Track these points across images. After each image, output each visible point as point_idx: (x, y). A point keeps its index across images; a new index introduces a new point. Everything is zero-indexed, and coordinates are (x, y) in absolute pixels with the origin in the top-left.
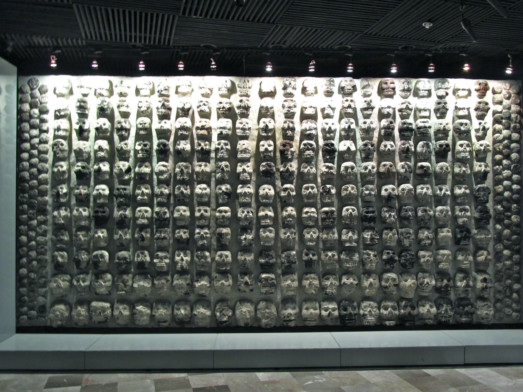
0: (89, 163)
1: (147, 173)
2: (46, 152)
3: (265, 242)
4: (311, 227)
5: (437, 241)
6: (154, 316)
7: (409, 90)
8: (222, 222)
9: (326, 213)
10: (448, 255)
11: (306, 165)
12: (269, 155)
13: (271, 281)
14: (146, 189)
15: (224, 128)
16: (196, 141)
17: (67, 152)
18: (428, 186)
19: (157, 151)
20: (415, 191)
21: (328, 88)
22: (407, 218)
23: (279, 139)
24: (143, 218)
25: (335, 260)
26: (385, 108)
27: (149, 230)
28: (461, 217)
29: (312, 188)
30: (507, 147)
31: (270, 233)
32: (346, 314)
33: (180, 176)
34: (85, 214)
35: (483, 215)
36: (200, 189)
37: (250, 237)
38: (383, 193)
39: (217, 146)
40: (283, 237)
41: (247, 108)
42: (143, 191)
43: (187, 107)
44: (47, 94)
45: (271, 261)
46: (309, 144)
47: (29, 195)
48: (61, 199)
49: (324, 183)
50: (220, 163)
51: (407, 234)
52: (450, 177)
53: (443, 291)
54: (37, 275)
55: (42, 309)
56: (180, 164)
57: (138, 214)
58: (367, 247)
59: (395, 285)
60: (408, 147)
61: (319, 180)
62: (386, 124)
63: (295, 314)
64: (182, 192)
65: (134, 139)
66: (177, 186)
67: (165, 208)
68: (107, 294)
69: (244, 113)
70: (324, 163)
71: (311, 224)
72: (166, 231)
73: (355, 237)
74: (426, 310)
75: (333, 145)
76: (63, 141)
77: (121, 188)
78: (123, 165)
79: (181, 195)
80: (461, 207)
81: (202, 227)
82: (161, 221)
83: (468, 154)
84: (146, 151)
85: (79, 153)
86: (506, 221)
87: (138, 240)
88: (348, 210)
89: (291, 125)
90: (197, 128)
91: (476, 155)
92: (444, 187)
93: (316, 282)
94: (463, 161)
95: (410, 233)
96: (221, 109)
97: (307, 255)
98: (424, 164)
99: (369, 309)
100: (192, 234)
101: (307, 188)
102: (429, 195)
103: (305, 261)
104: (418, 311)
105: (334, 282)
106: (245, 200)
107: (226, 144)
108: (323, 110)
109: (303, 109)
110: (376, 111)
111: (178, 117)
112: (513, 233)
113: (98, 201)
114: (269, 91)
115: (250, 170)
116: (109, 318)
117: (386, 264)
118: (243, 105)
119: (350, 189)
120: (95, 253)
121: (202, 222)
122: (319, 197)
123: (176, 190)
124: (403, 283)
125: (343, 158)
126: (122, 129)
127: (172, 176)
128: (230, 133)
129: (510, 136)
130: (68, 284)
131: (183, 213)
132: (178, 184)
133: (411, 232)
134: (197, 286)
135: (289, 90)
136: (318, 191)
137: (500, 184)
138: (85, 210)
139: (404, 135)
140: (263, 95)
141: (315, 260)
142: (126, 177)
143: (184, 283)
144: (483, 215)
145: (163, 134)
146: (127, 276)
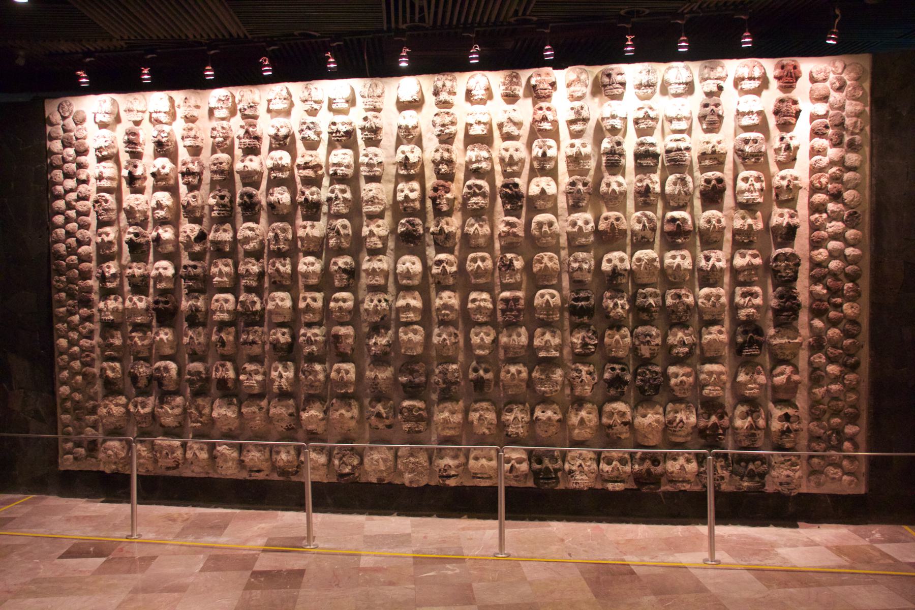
0: (145, 228)
1: (226, 242)
2: (87, 214)
3: (407, 349)
4: (481, 324)
5: (702, 349)
6: (243, 461)
7: (649, 85)
8: (340, 317)
9: (506, 301)
10: (721, 373)
12: (412, 207)
13: (417, 411)
14: (226, 265)
15: (339, 165)
16: (299, 186)
17: (115, 212)
18: (685, 252)
19: (239, 205)
20: (662, 262)
21: (507, 89)
22: (647, 309)
23: (430, 178)
24: (222, 311)
25: (522, 380)
26: (608, 118)
27: (232, 329)
28: (743, 307)
29: (483, 259)
30: (835, 179)
32: (540, 469)
34: (142, 305)
35: (785, 303)
36: (305, 264)
37: (383, 341)
38: (606, 266)
39: (331, 195)
41: (376, 130)
42: (220, 270)
43: (283, 132)
44: (85, 125)
45: (417, 380)
46: (476, 186)
47: (67, 278)
48: (108, 284)
49: (505, 249)
51: (646, 336)
52: (728, 236)
53: (707, 435)
54: (83, 396)
55: (93, 447)
57: (214, 306)
58: (582, 357)
59: (625, 424)
60: (647, 185)
61: (497, 245)
62: (609, 146)
63: (457, 467)
64: (278, 270)
65: (208, 187)
66: (271, 261)
67: (254, 295)
68: (176, 427)
69: (371, 139)
70: (506, 216)
71: (481, 318)
72: (255, 332)
73: (556, 341)
74: (678, 467)
75: (516, 185)
76: (107, 196)
77: (190, 266)
78: (189, 229)
79: (277, 275)
80: (745, 289)
81: (309, 325)
82: (248, 316)
83: (757, 194)
84: (224, 206)
85: (130, 213)
86: (832, 314)
87: (217, 345)
88: (546, 296)
89: (446, 155)
90: (299, 166)
91: (777, 195)
92: (713, 255)
93: (491, 416)
94: (748, 207)
95: (651, 336)
96: (334, 135)
97: (476, 370)
98: (676, 214)
99: (579, 462)
100: (294, 337)
101: (474, 260)
102: (685, 269)
103: (472, 380)
104: (665, 469)
105: (520, 416)
107: (343, 191)
108: (501, 126)
109: (468, 126)
110: (592, 124)
111: (271, 149)
112: (847, 334)
113: (158, 286)
114: (410, 99)
116: (180, 462)
117: (609, 387)
118: (368, 125)
119: (546, 260)
120: (158, 364)
121: (309, 317)
122: (497, 274)
124: (639, 420)
125: (536, 207)
126: (188, 173)
128: (350, 172)
129: (843, 158)
130: (123, 410)
131: (280, 304)
133: (654, 333)
134: (304, 418)
135: (444, 96)
136: (494, 263)
137: (821, 247)
138: (141, 300)
139: (641, 165)
140: (403, 106)
141: (488, 380)
142: (197, 248)
143: (284, 413)
145: (251, 178)
146: (203, 401)
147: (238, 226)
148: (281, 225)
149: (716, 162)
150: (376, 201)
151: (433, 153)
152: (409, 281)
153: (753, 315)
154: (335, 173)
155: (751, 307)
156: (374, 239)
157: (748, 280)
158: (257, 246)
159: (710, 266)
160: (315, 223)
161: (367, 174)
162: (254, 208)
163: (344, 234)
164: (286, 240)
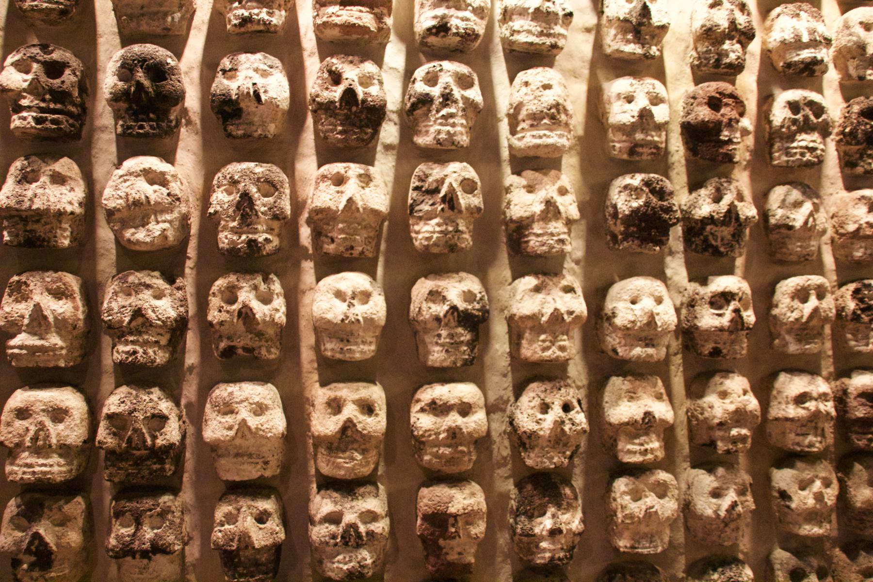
8: (450, 461)
11: (796, 194)
14: (59, 294)
19: (116, 98)
24: (40, 448)
27: (77, 506)
31: (662, 496)
33: (233, 230)
36: (339, 295)
39: (420, 87)
40: (709, 512)
42: (38, 307)
46: (811, 104)
50: (436, 172)
56: (235, 169)
61: (829, 260)
64: (246, 314)
72: (163, 514)
79: (241, 327)
82: (139, 462)
84: (60, 96)
89: (741, 20)
101: (802, 295)
106: (553, 353)
107: (464, 82)
115: (569, 206)
123: (215, 302)
127: (194, 230)
131: (253, 422)
132: (224, 272)
147: (99, 171)
148: (259, 169)
150: (563, 117)
151: (706, 9)
152: (650, 351)
154: (442, 28)
156: (557, 227)
158: (171, 234)
160: (370, 168)
161: (535, 40)
162: (167, 112)
163: (469, 208)
164: (275, 217)
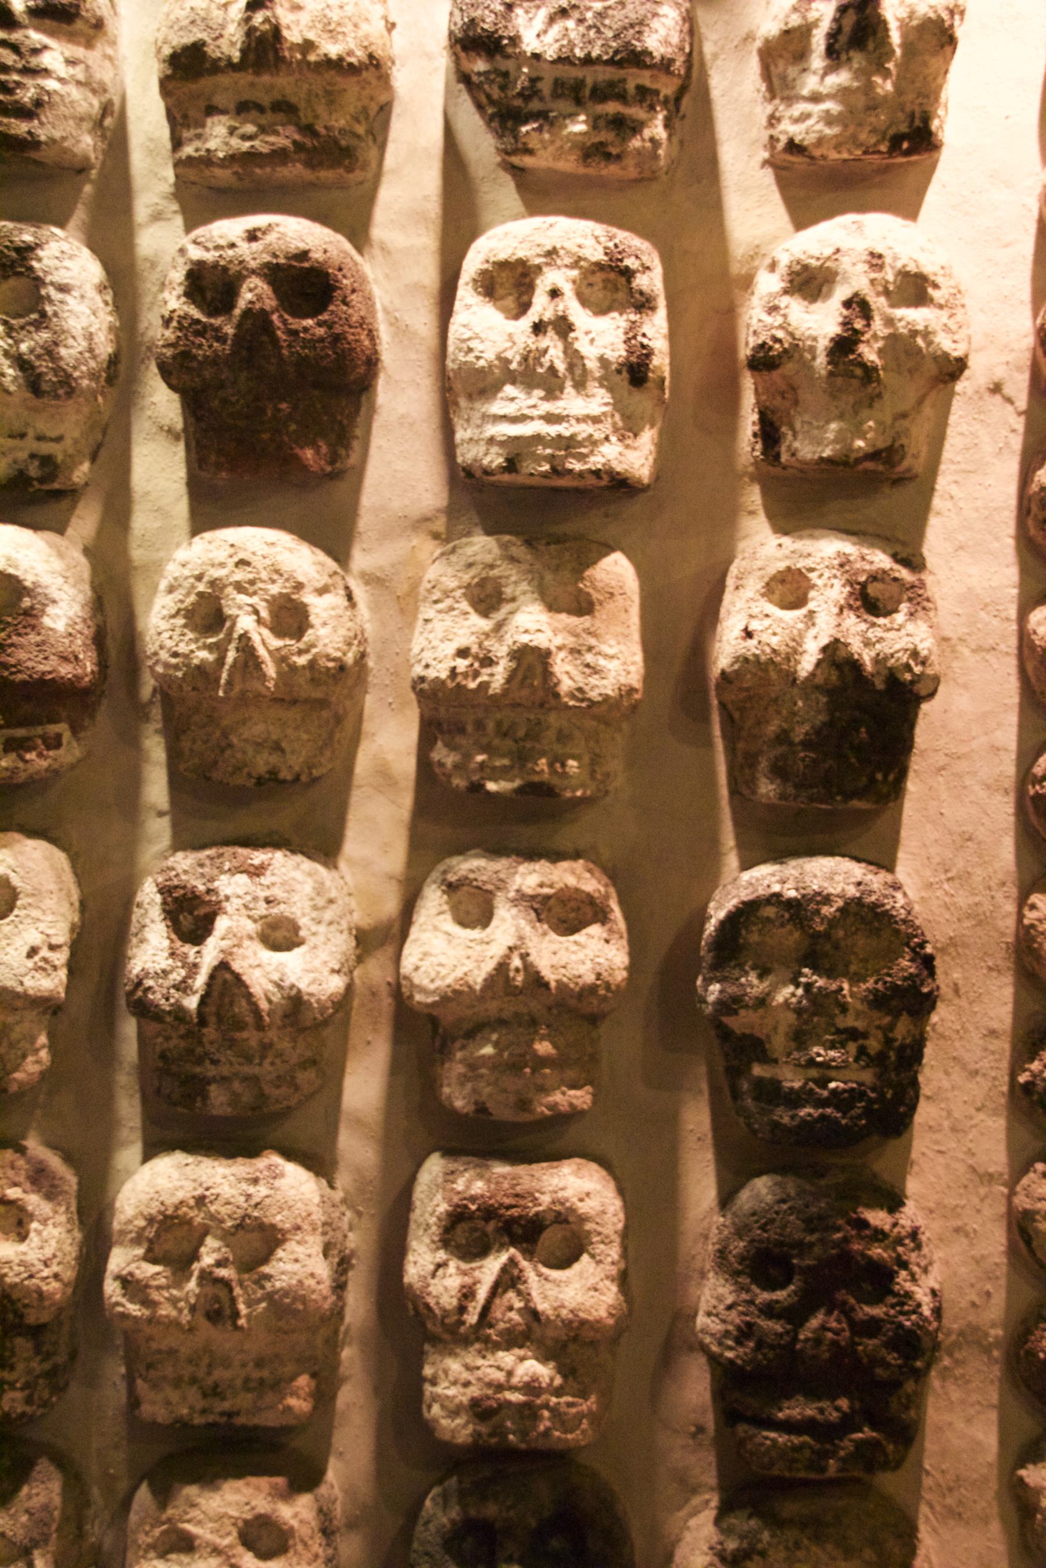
35: (795, 1315)
144: (795, 1315)
149: (283, 138)
153: (528, 1412)
155: (512, 1340)
157: (503, 1113)
159: (200, 981)
